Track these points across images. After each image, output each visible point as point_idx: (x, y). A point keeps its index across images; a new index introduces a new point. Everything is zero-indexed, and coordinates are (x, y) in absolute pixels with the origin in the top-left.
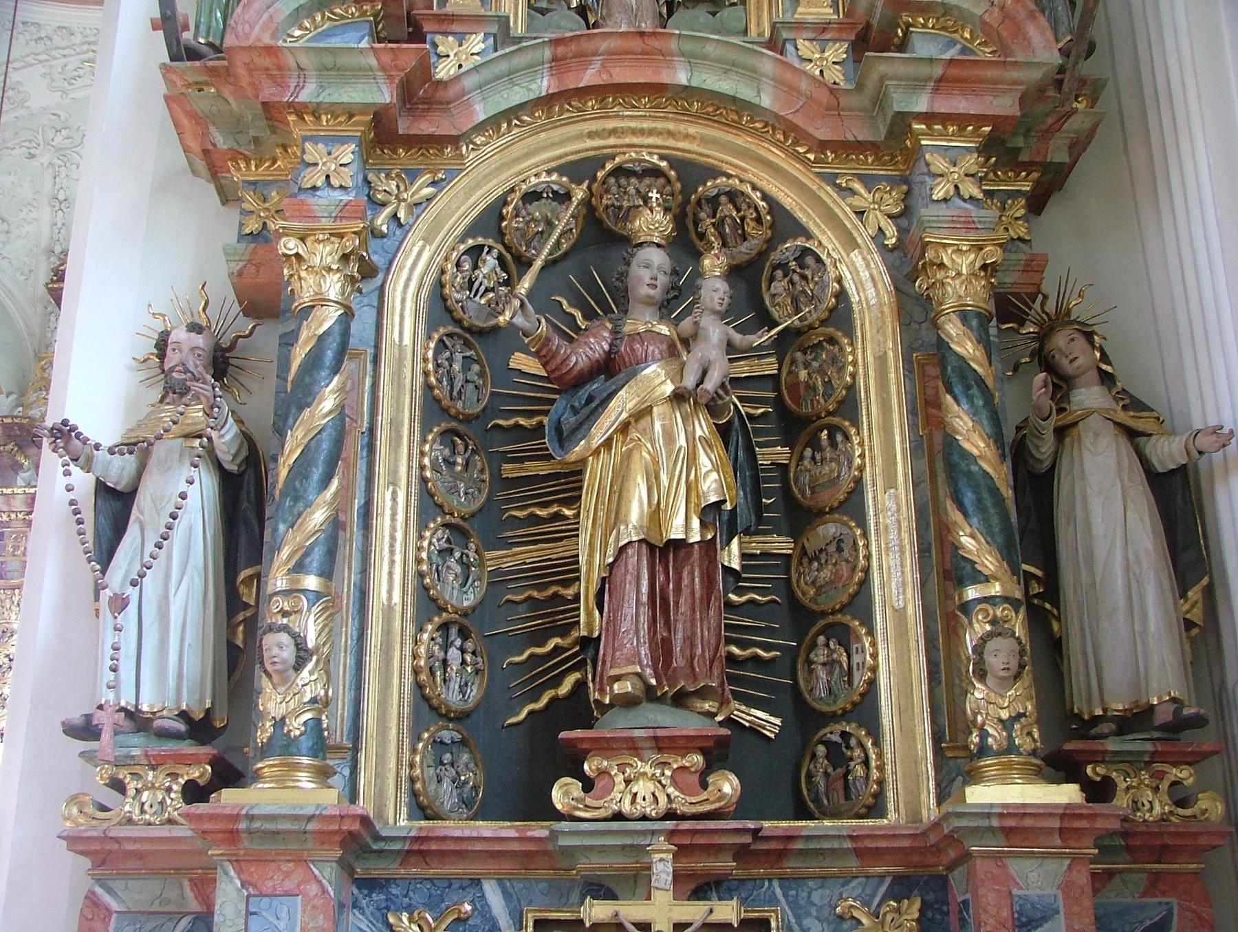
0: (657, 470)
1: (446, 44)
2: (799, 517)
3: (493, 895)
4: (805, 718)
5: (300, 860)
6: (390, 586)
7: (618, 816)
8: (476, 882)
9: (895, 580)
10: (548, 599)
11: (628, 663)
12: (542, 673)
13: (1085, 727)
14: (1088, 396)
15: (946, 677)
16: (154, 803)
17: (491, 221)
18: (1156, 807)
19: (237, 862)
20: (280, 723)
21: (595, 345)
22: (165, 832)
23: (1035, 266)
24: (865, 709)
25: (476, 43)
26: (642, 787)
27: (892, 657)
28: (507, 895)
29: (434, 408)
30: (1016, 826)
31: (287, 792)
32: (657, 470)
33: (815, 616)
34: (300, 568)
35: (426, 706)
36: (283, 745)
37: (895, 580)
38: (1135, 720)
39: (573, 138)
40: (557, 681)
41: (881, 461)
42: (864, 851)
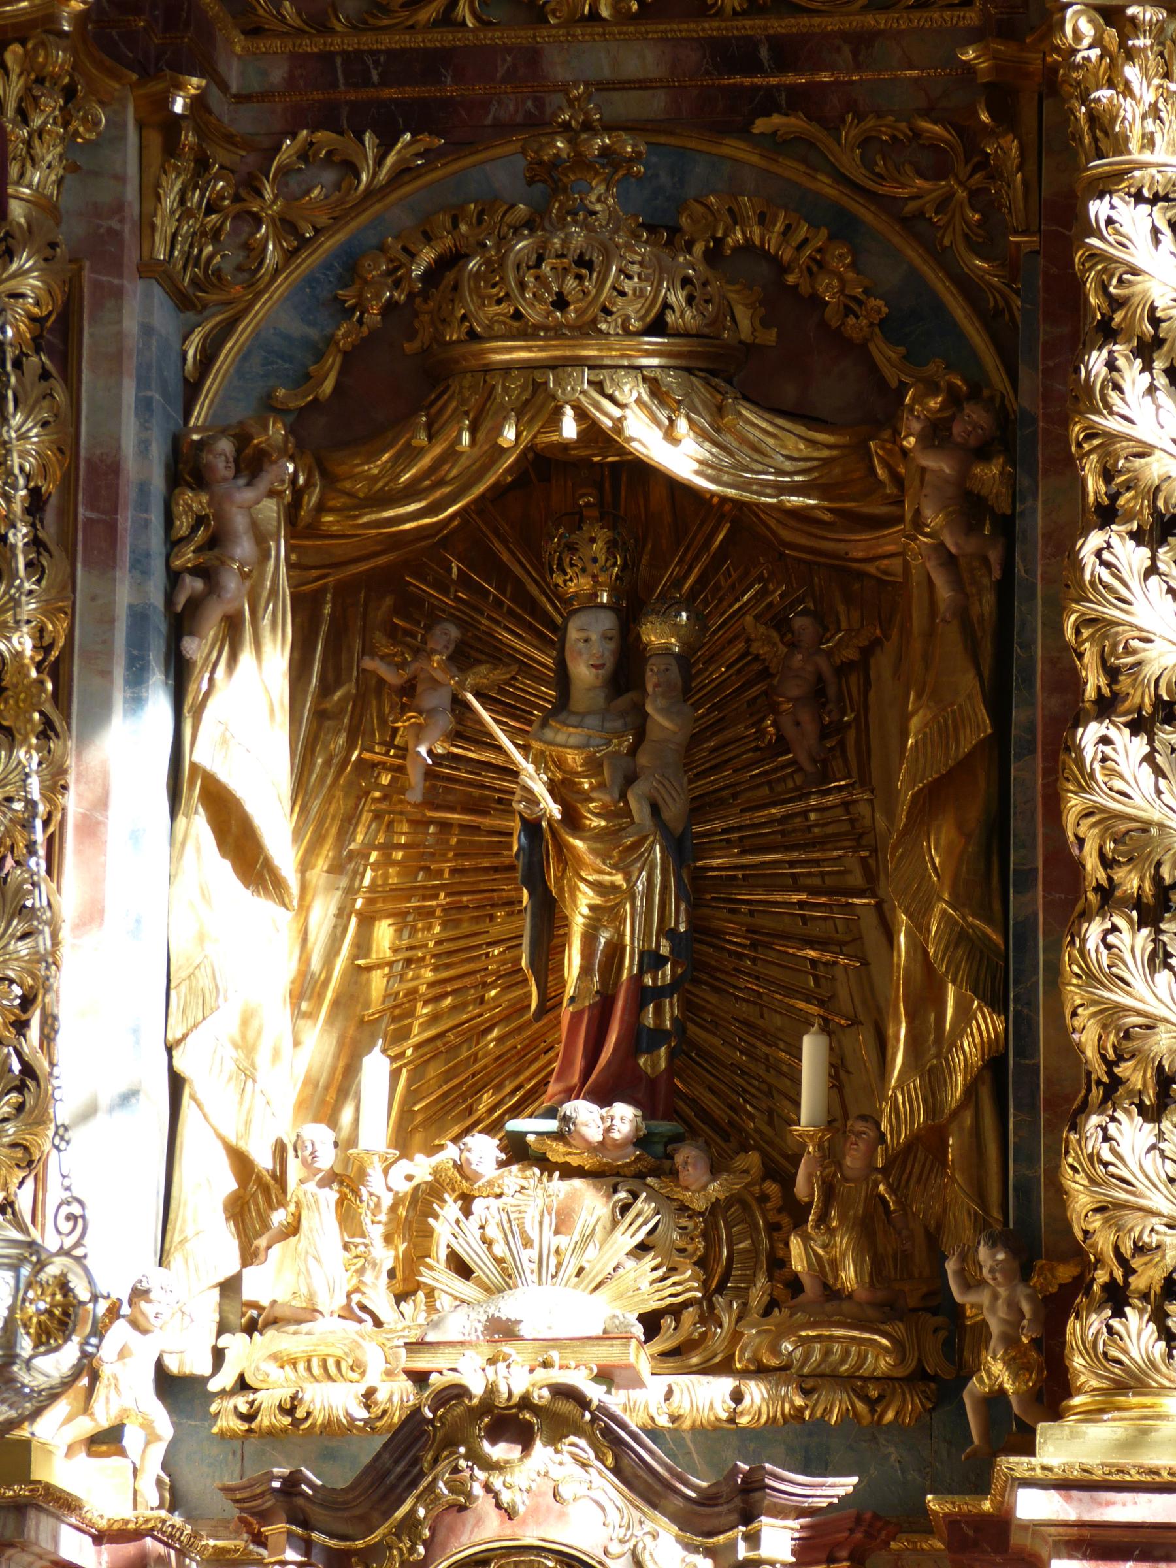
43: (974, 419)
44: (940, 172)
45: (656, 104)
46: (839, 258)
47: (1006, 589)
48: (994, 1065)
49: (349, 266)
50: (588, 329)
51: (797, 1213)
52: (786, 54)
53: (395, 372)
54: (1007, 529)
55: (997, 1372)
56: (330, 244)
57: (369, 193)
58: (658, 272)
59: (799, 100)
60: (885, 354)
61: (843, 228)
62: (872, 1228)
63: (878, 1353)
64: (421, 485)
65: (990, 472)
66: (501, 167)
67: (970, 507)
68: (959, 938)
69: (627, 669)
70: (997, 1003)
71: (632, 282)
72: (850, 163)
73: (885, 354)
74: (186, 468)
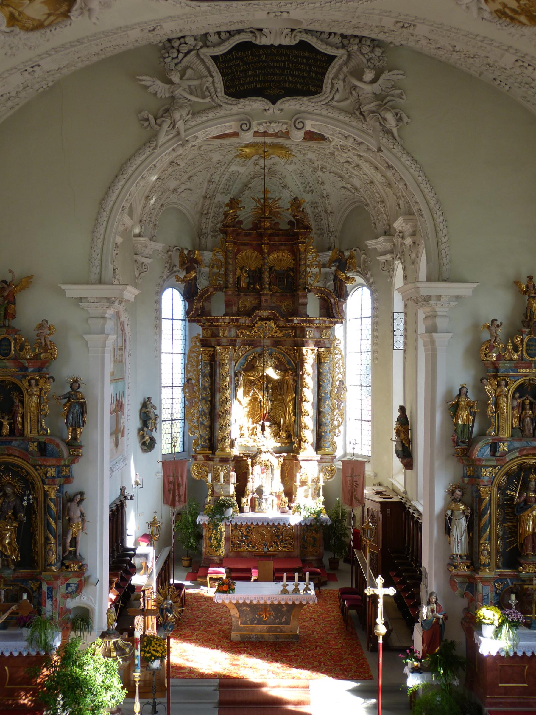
1: (501, 444)
3: (509, 580)
5: (489, 581)
7: (528, 573)
8: (506, 579)
12: (511, 543)
16: (463, 569)
19: (481, 582)
20: (484, 562)
22: (465, 573)
25: (505, 444)
28: (511, 580)
31: (487, 573)
34: (486, 540)
36: (485, 565)
40: (513, 545)
43: (294, 374)
44: (291, 351)
45: (270, 344)
46: (283, 358)
47: (296, 386)
48: (295, 420)
49: (247, 357)
50: (266, 367)
51: (280, 431)
52: (280, 341)
53: (251, 367)
54: (296, 382)
55: (295, 445)
56: (245, 355)
57: (248, 351)
58: (271, 361)
59: (281, 345)
60: (287, 365)
61: (284, 355)
62: (286, 431)
63: (286, 441)
64: (253, 376)
65: (295, 377)
66: (258, 349)
67: (294, 380)
68: (292, 411)
69: (267, 387)
70: (295, 416)
71: (270, 363)
72: (284, 350)
73: (287, 365)
74: (236, 375)
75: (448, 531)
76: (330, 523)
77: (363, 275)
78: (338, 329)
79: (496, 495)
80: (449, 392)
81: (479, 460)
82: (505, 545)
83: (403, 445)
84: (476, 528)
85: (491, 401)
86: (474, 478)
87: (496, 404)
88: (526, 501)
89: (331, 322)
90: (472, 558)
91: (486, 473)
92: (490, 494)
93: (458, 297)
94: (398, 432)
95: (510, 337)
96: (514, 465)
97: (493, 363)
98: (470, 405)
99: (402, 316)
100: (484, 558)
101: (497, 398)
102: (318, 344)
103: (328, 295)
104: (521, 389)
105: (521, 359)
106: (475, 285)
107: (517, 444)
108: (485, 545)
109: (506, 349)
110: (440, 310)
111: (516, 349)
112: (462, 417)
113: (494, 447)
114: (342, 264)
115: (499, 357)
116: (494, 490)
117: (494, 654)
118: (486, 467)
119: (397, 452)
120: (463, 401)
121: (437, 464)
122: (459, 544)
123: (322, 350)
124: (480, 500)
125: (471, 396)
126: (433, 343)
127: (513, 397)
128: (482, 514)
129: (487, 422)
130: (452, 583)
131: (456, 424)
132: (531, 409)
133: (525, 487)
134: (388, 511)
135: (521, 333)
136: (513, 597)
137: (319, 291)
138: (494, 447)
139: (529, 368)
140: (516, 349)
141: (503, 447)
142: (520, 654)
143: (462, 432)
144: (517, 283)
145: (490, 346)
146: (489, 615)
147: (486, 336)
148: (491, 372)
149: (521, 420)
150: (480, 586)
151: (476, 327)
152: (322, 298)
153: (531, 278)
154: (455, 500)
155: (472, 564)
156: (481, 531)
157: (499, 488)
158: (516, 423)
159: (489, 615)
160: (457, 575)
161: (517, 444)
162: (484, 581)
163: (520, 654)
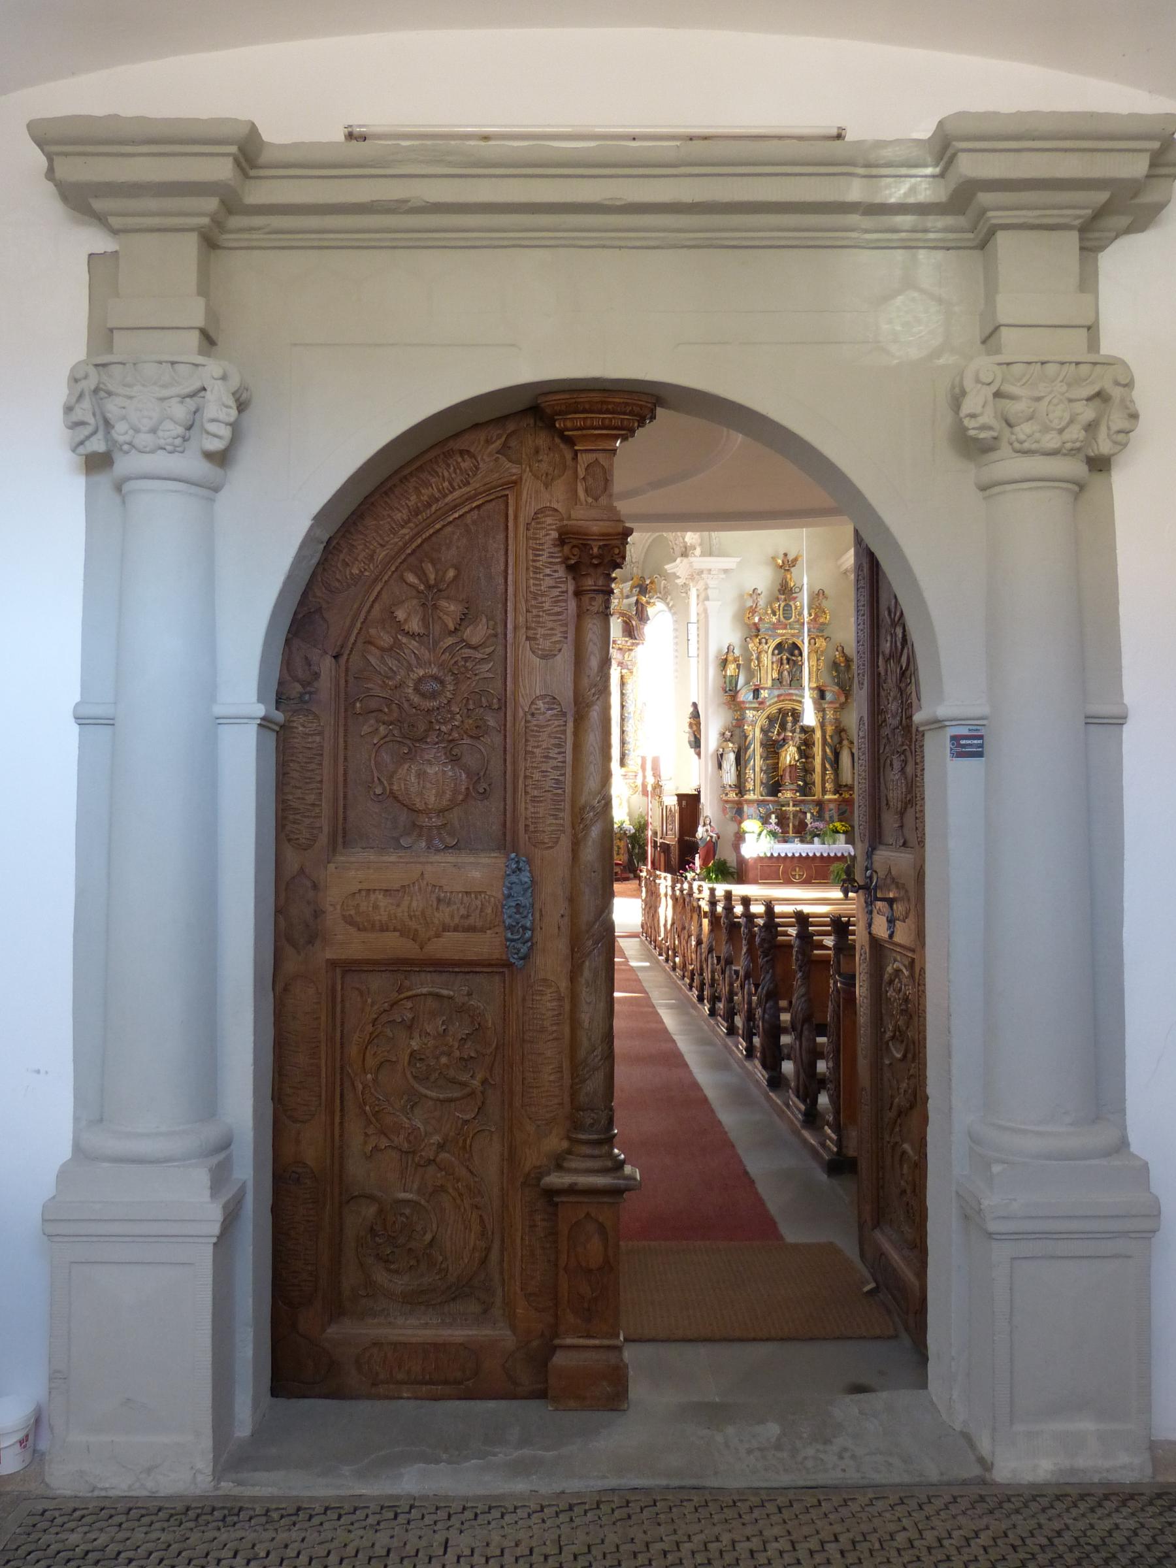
0: (790, 755)
2: (807, 757)
4: (806, 784)
6: (757, 769)
9: (818, 768)
10: (775, 767)
11: (787, 779)
12: (774, 777)
13: (840, 786)
14: (845, 742)
15: (824, 782)
16: (732, 796)
17: (768, 717)
18: (847, 796)
21: (782, 737)
23: (840, 723)
24: (814, 783)
26: (789, 795)
27: (817, 777)
29: (762, 744)
30: (830, 801)
31: (751, 796)
32: (790, 755)
33: (807, 770)
35: (762, 783)
37: (818, 768)
38: (846, 786)
39: (779, 706)
41: (818, 750)
42: (813, 801)
75: (720, 766)
76: (633, 831)
77: (663, 599)
78: (639, 650)
79: (758, 734)
80: (720, 651)
81: (743, 702)
82: (769, 779)
83: (695, 736)
84: (742, 762)
85: (754, 657)
86: (739, 722)
87: (758, 659)
88: (784, 739)
89: (633, 644)
90: (740, 788)
91: (750, 714)
92: (755, 735)
93: (726, 571)
94: (691, 725)
95: (770, 603)
96: (774, 710)
97: (755, 624)
98: (736, 660)
99: (695, 626)
100: (750, 786)
101: (759, 653)
102: (620, 664)
103: (630, 618)
104: (779, 646)
105: (779, 620)
106: (738, 559)
107: (776, 692)
108: (749, 773)
109: (766, 613)
110: (712, 583)
111: (774, 613)
112: (731, 669)
113: (756, 692)
114: (643, 589)
115: (760, 619)
116: (758, 730)
117: (755, 856)
118: (750, 709)
119: (690, 742)
120: (730, 658)
121: (710, 711)
122: (729, 777)
123: (624, 671)
124: (746, 737)
125: (737, 652)
126: (705, 611)
127: (773, 654)
128: (747, 748)
129: (751, 674)
130: (724, 810)
131: (725, 677)
132: (788, 663)
133: (783, 727)
134: (684, 803)
135: (778, 600)
136: (773, 816)
137: (622, 615)
138: (756, 692)
139: (785, 628)
140: (774, 613)
141: (764, 694)
142: (775, 855)
143: (730, 682)
144: (774, 558)
145: (753, 611)
146: (751, 826)
147: (749, 603)
148: (754, 632)
149: (780, 673)
150: (745, 807)
151: (741, 597)
152: (625, 622)
153: (786, 555)
154: (726, 740)
155: (740, 792)
156: (747, 762)
157: (762, 730)
158: (775, 675)
159: (751, 826)
160: (727, 802)
161: (776, 692)
162: (749, 802)
163: (775, 855)
